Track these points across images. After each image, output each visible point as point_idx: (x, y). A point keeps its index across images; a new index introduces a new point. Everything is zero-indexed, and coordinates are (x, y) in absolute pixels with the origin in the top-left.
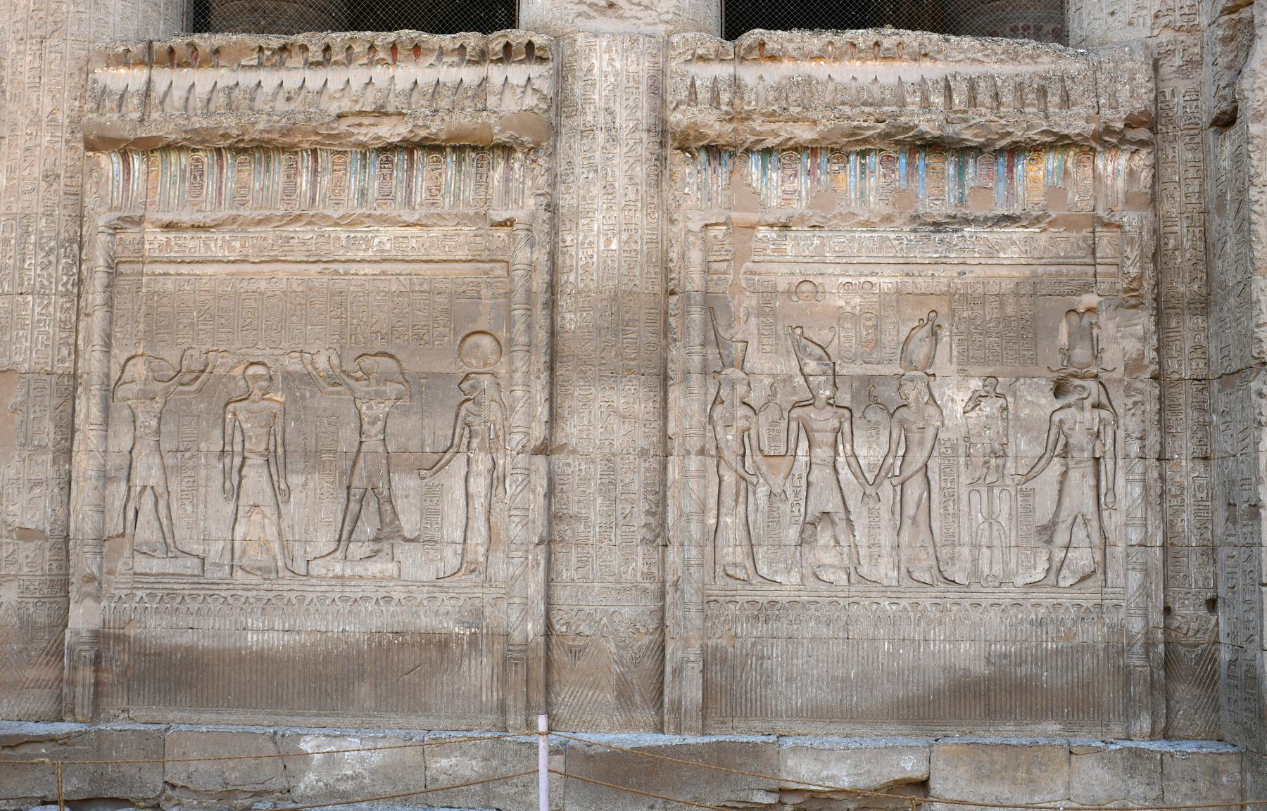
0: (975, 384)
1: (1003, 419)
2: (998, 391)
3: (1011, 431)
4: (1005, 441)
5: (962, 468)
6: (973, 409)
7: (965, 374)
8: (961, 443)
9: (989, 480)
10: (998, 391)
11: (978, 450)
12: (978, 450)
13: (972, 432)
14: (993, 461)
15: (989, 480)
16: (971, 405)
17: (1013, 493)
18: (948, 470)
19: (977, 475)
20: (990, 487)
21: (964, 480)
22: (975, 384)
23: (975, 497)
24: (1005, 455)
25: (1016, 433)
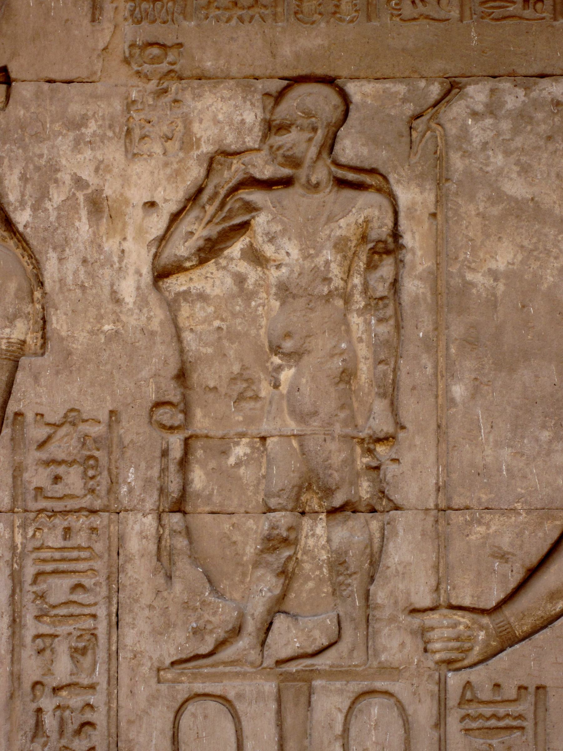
0: (224, 116)
1: (375, 303)
2: (350, 148)
3: (417, 369)
4: (381, 423)
5: (139, 571)
6: (210, 250)
7: (166, 69)
8: (134, 429)
9: (287, 638)
10: (350, 148)
11: (241, 476)
12: (241, 476)
13: (206, 376)
14: (318, 536)
15: (287, 638)
16: (197, 229)
17: (423, 712)
18: (59, 589)
19: (222, 616)
20: (295, 678)
21: (147, 641)
22: (224, 116)
23: (209, 731)
24: (384, 504)
25: (445, 372)
